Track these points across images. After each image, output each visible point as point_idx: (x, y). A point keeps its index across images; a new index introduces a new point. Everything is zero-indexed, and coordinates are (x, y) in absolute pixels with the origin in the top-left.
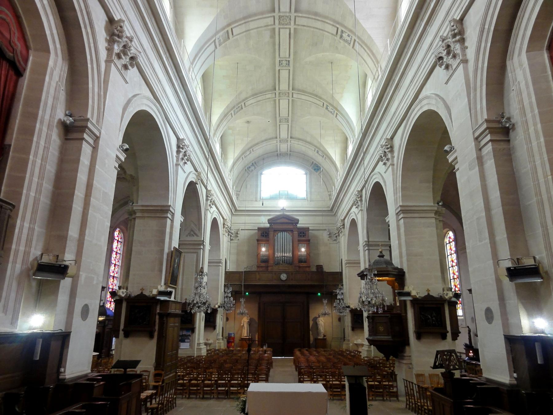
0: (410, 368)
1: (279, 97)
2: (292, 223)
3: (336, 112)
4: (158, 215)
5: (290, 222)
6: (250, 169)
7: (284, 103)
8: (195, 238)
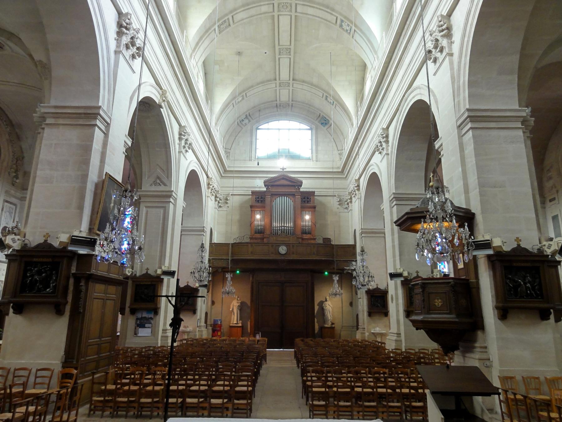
0: (487, 367)
1: (279, 11)
2: (294, 186)
3: (353, 28)
4: (81, 122)
5: (291, 184)
6: (243, 123)
7: (285, 21)
8: (162, 188)
